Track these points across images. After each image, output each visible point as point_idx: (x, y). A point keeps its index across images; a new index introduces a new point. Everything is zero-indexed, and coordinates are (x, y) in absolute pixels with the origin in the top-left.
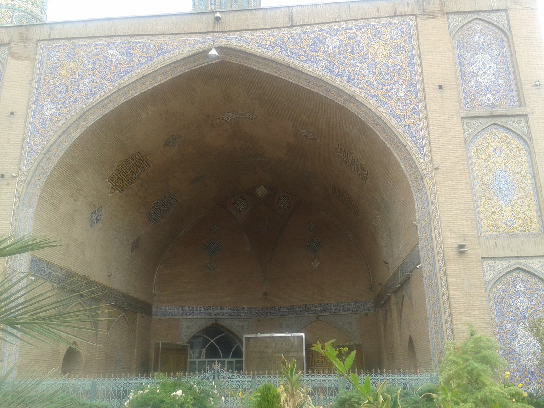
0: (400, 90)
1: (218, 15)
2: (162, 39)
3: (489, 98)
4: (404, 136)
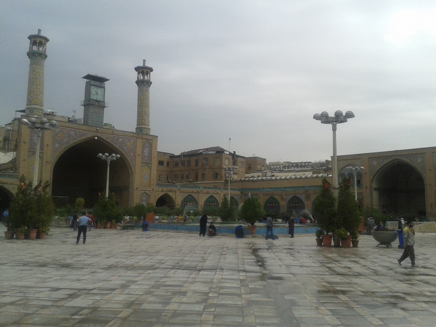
0: (132, 154)
1: (98, 128)
2: (84, 131)
3: (146, 158)
4: (131, 164)
